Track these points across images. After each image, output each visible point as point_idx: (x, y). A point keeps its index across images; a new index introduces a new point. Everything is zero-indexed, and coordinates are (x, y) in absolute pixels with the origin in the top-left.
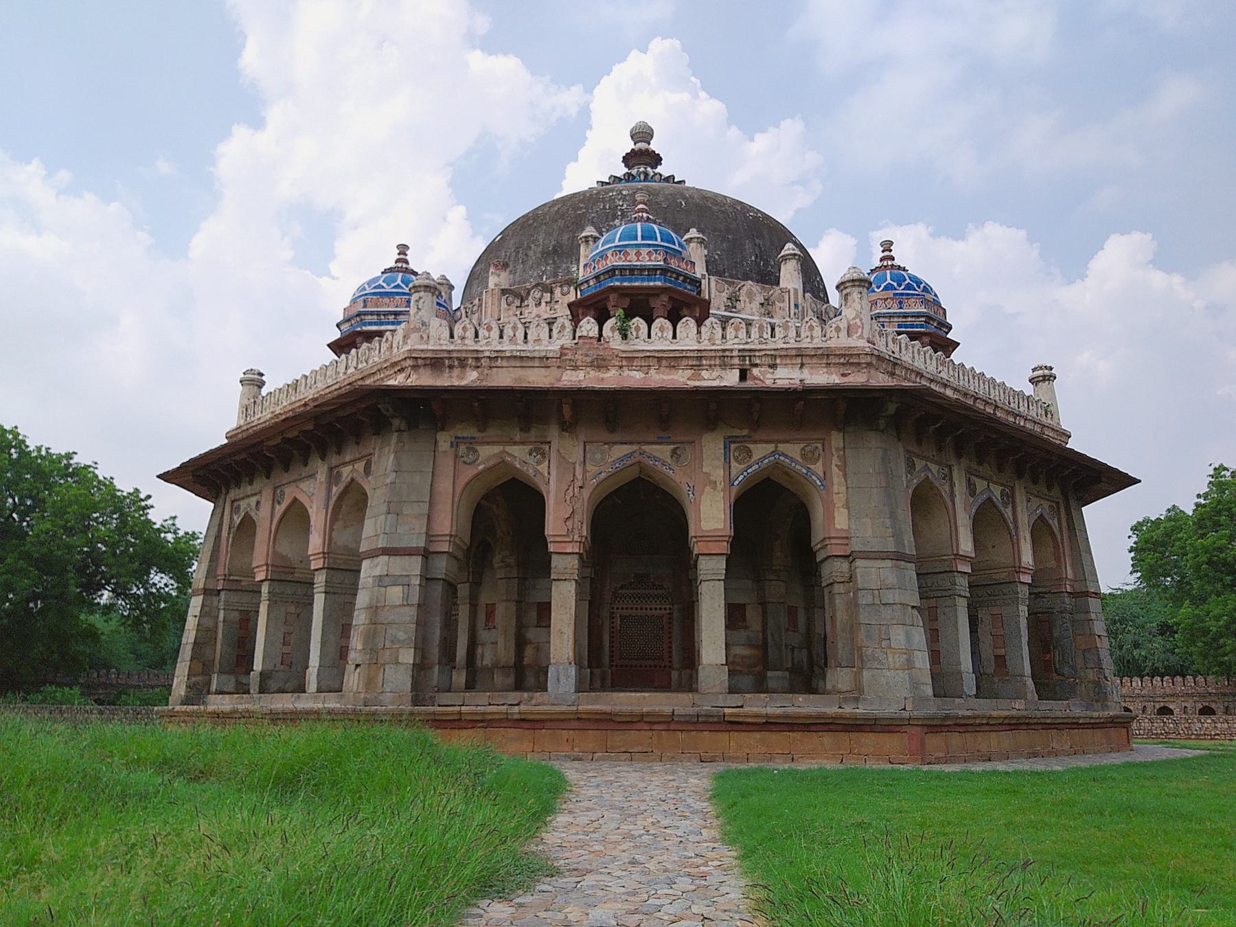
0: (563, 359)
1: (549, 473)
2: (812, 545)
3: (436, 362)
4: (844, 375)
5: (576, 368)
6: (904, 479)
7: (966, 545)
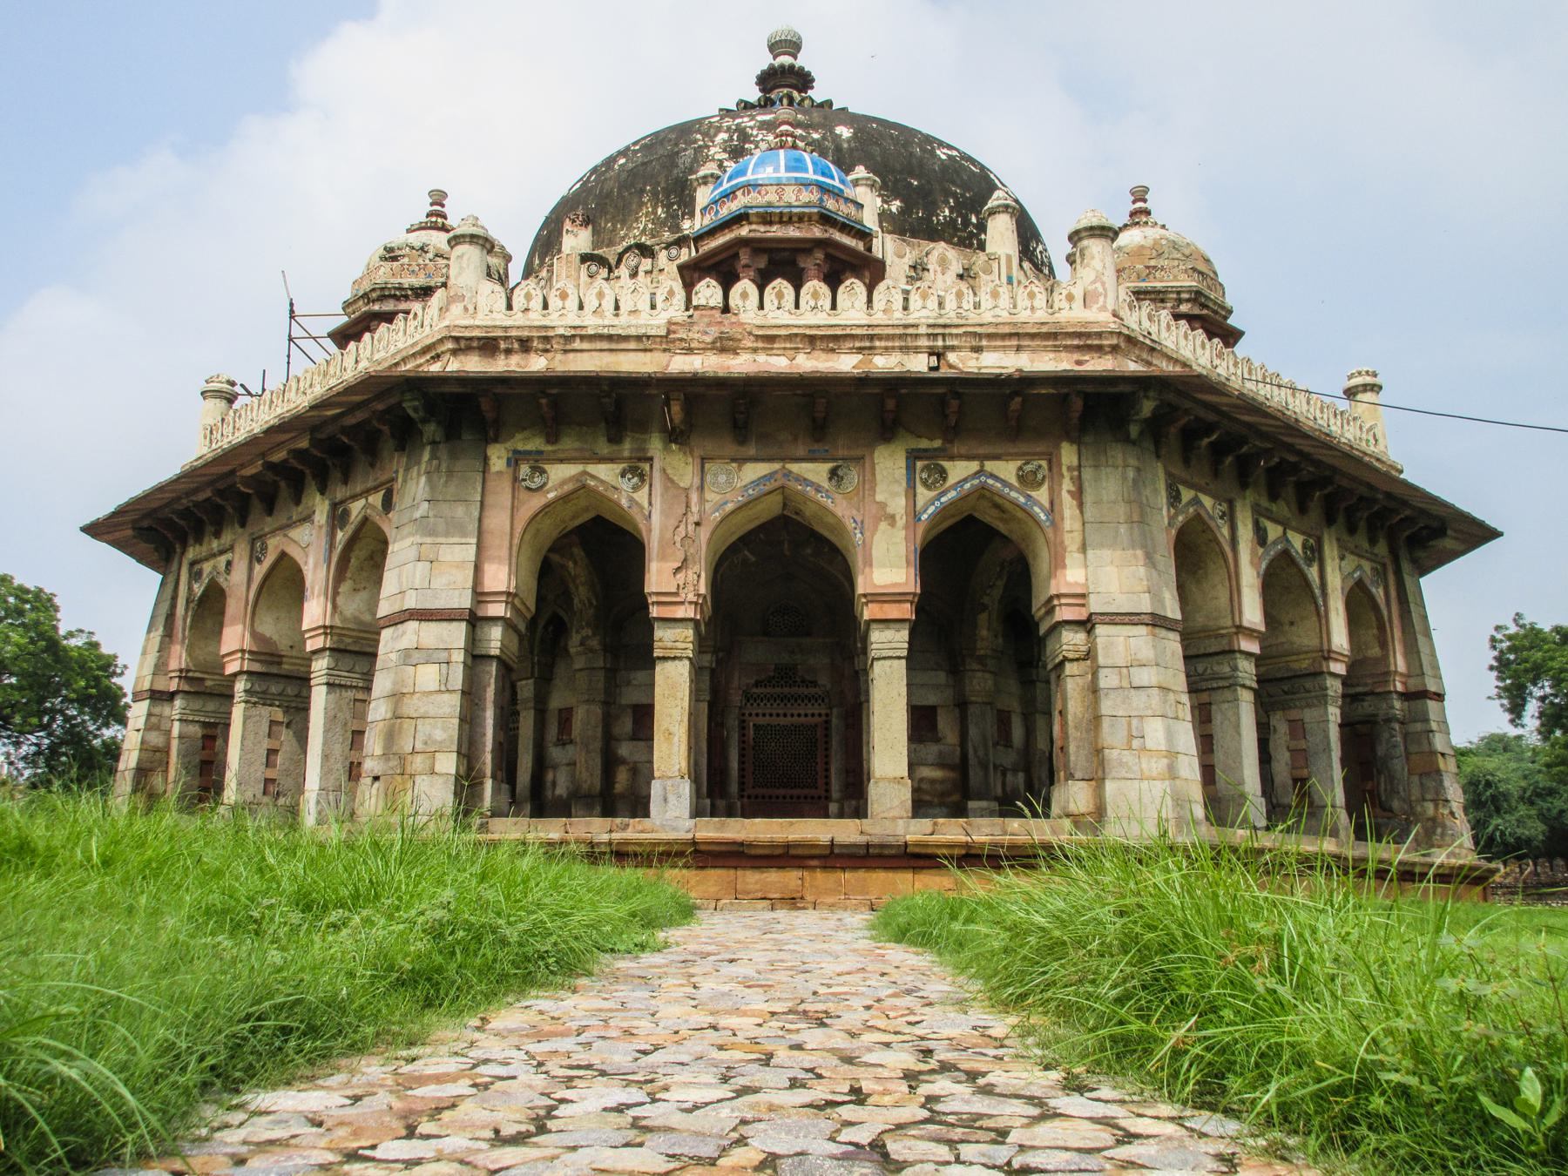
0: (668, 341)
1: (650, 504)
2: (1034, 610)
3: (488, 345)
4: (1079, 363)
5: (690, 351)
6: (1165, 512)
7: (1252, 613)
